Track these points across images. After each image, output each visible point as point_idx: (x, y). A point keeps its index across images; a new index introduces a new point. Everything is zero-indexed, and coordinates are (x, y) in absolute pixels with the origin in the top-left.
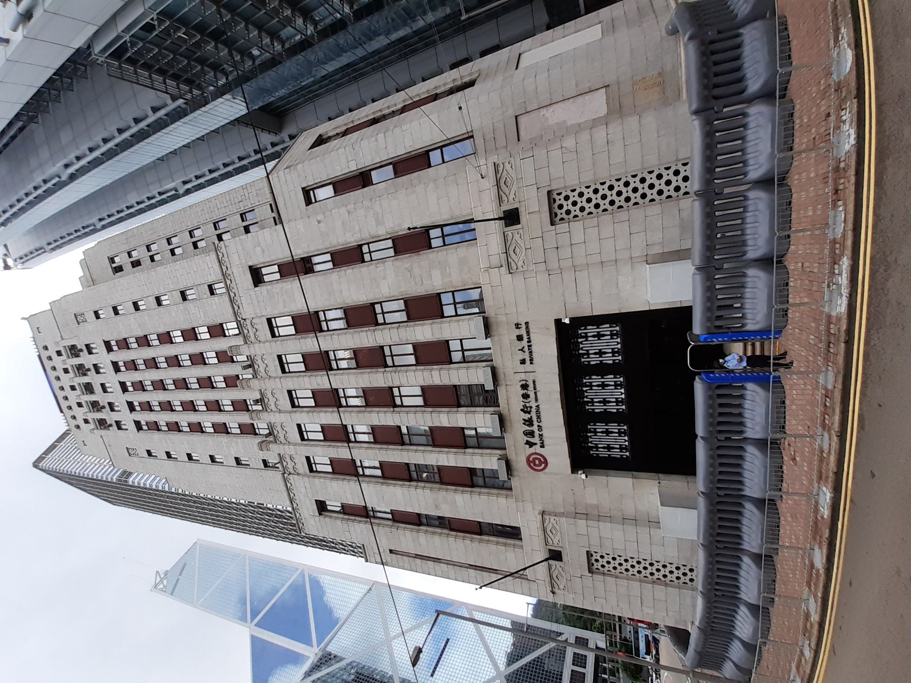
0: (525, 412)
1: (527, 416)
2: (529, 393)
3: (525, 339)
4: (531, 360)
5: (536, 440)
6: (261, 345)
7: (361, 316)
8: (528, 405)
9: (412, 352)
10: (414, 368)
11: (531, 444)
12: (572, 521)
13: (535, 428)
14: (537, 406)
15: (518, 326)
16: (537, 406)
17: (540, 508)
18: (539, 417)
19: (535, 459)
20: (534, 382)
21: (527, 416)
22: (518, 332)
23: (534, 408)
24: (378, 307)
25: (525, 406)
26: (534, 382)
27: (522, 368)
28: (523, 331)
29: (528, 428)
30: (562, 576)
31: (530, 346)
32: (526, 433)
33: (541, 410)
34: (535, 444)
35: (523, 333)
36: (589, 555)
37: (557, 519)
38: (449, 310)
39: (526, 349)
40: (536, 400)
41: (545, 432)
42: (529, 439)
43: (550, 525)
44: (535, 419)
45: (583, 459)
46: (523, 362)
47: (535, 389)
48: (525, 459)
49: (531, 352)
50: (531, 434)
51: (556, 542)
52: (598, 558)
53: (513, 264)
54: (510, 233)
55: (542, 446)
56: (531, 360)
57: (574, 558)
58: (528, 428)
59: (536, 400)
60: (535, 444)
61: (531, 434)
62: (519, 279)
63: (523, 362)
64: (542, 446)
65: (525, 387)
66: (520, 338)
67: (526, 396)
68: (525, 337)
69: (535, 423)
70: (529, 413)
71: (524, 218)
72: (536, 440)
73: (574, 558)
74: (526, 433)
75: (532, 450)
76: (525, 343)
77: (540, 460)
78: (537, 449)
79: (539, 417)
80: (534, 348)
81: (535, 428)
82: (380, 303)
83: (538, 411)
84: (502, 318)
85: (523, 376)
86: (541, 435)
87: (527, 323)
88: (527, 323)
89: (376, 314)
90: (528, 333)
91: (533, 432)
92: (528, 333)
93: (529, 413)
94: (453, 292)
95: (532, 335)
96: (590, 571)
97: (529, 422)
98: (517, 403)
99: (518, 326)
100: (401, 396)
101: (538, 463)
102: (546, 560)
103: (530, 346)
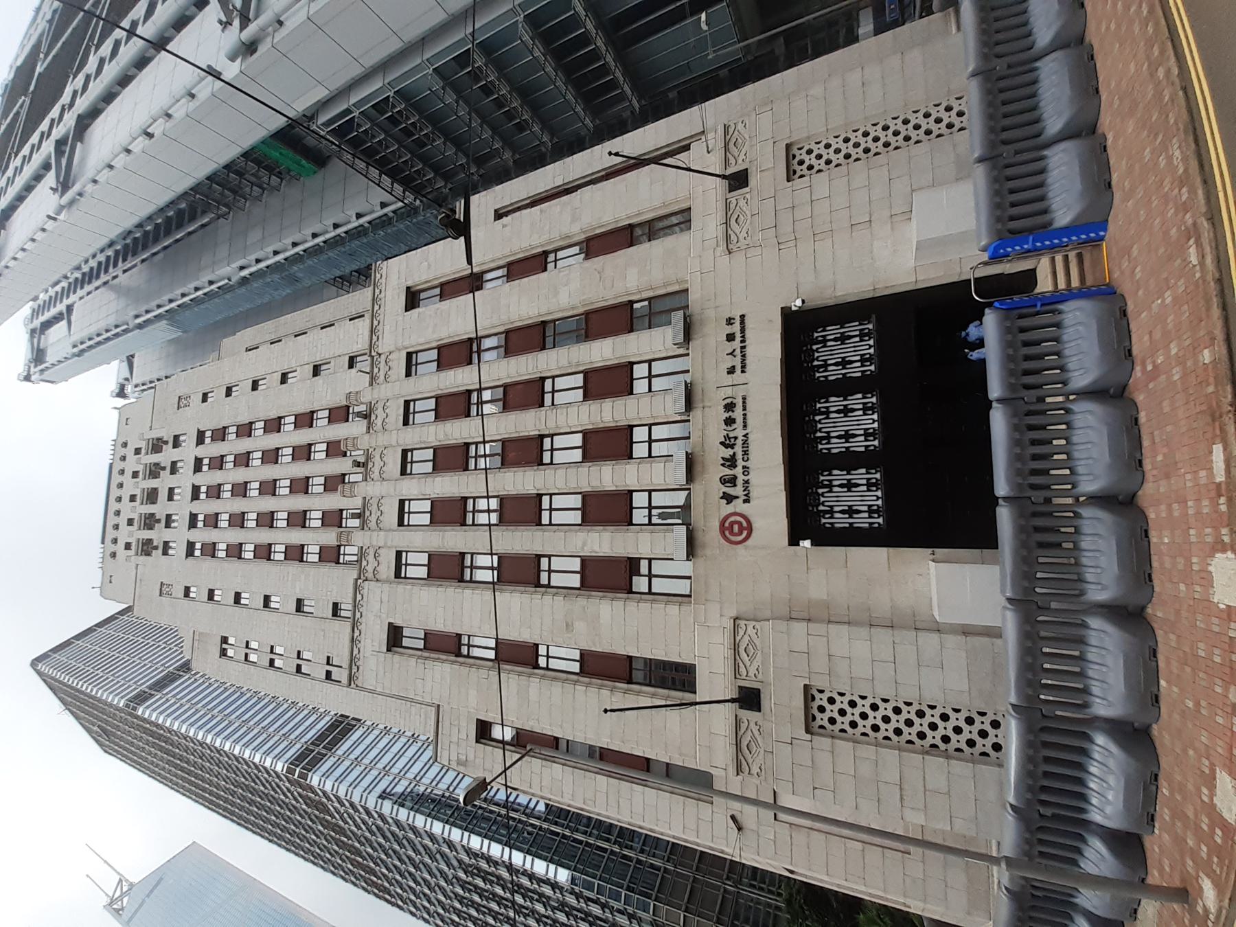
0: (727, 446)
1: (730, 452)
3: (738, 339)
4: (743, 366)
5: (738, 491)
6: (379, 584)
7: (521, 572)
8: (731, 435)
9: (578, 569)
10: (575, 677)
11: (729, 498)
12: (782, 625)
15: (730, 321)
17: (734, 614)
18: (746, 453)
19: (732, 524)
20: (744, 398)
22: (729, 330)
23: (741, 438)
24: (544, 561)
25: (727, 437)
26: (744, 398)
27: (729, 380)
28: (736, 328)
30: (758, 746)
31: (743, 348)
32: (723, 481)
34: (737, 497)
35: (737, 331)
36: (808, 695)
37: (758, 625)
38: (639, 516)
39: (738, 352)
40: (745, 426)
42: (731, 491)
43: (746, 638)
44: (739, 456)
45: (805, 522)
46: (731, 371)
48: (716, 524)
49: (744, 356)
51: (752, 672)
52: (825, 704)
53: (733, 237)
54: (734, 200)
55: (746, 501)
56: (743, 366)
57: (784, 702)
59: (745, 426)
60: (737, 497)
61: (732, 481)
62: (739, 257)
63: (731, 371)
65: (730, 407)
66: (730, 338)
67: (729, 421)
68: (738, 335)
69: (740, 463)
70: (732, 446)
71: (753, 181)
72: (738, 491)
73: (784, 702)
74: (723, 481)
75: (730, 509)
76: (737, 344)
77: (740, 524)
78: (738, 506)
79: (746, 453)
80: (748, 351)
82: (549, 557)
83: (745, 442)
84: (711, 313)
85: (729, 392)
86: (747, 482)
87: (742, 317)
88: (742, 317)
89: (539, 571)
90: (743, 330)
91: (735, 478)
92: (743, 330)
93: (732, 446)
94: (650, 492)
95: (748, 334)
96: (808, 731)
97: (731, 462)
98: (716, 432)
99: (730, 321)
100: (548, 657)
101: (737, 530)
102: (732, 701)
103: (743, 348)
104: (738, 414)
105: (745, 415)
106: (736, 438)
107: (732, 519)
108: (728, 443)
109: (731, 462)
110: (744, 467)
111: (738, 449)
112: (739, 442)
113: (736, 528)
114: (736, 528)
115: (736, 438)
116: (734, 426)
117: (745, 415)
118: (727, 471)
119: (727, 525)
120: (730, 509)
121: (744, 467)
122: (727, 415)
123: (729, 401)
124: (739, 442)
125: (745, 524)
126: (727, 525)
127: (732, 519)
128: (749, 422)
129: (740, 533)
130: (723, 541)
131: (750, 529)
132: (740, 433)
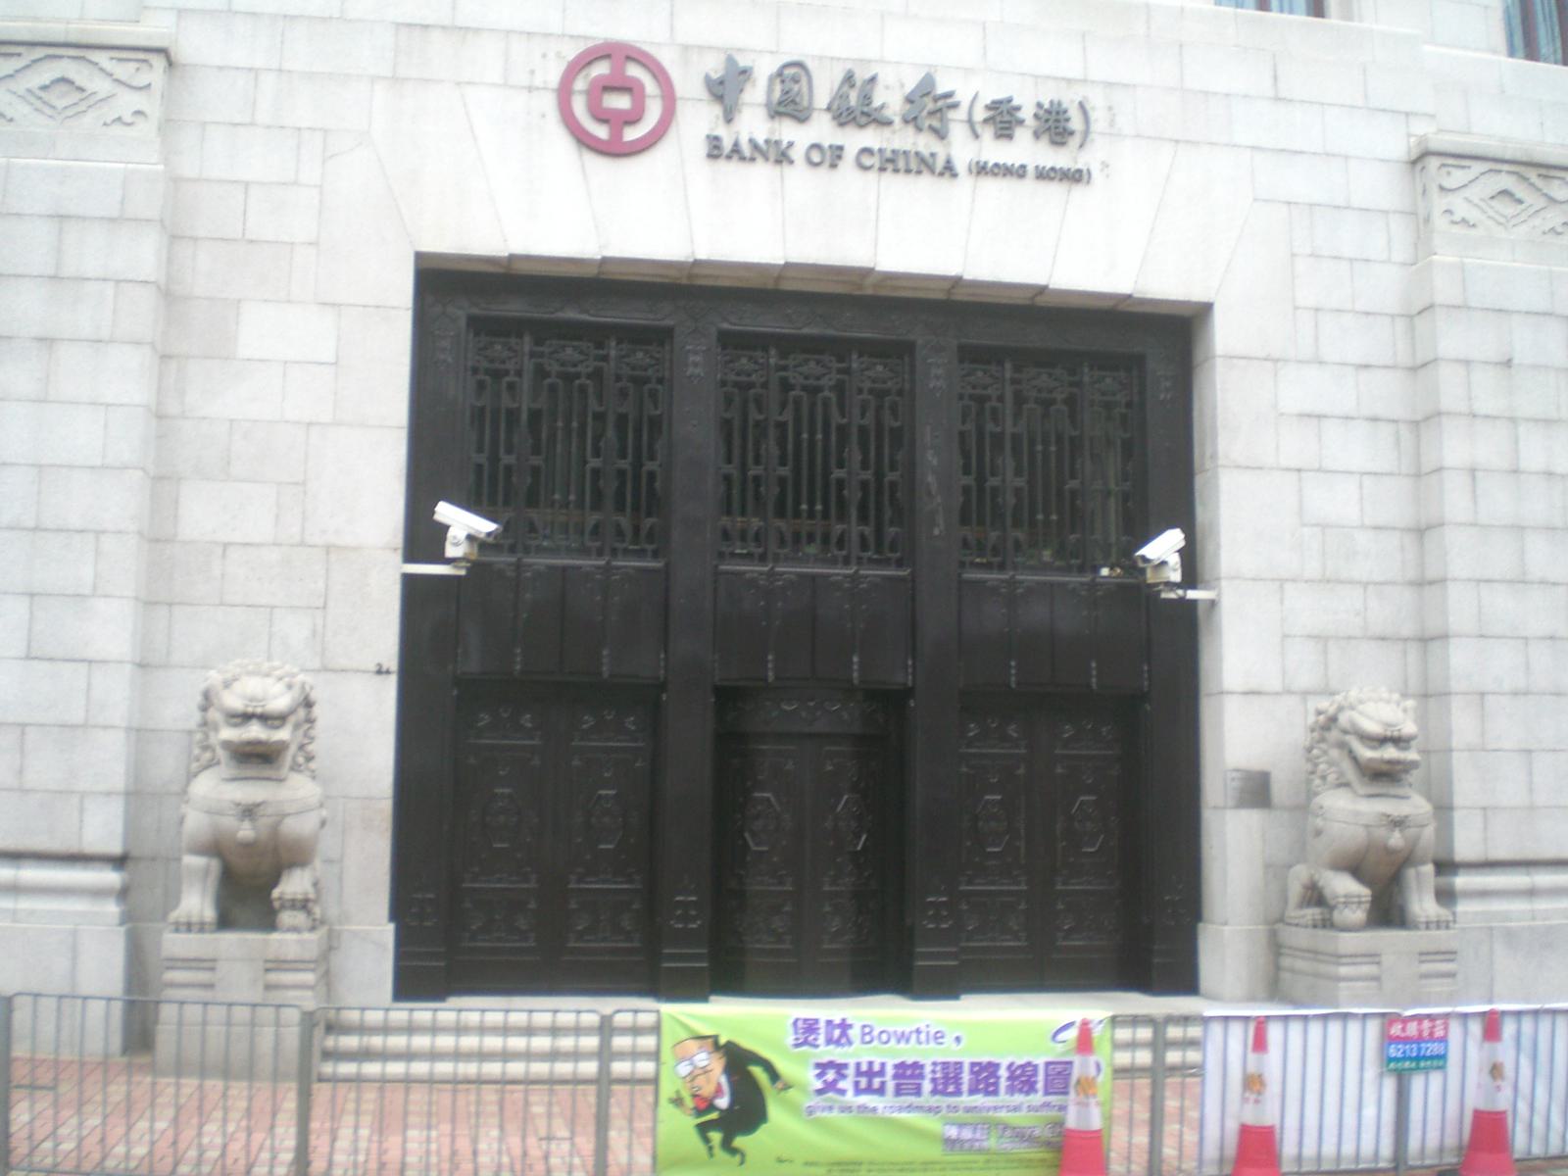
2: (1023, 136)
11: (725, 90)
13: (821, 129)
14: (949, 170)
16: (949, 170)
18: (891, 162)
20: (1074, 177)
21: (890, 98)
25: (945, 104)
29: (822, 96)
33: (926, 181)
34: (729, 118)
40: (981, 170)
41: (798, 177)
42: (756, 94)
47: (1044, 175)
50: (789, 106)
55: (715, 149)
58: (822, 96)
59: (981, 170)
60: (729, 118)
61: (789, 106)
64: (715, 149)
65: (1055, 126)
67: (1003, 119)
69: (855, 140)
72: (753, 124)
77: (633, 118)
78: (697, 119)
81: (821, 129)
83: (924, 165)
86: (781, 156)
104: (1024, 149)
105: (1020, 172)
106: (941, 134)
107: (650, 86)
108: (929, 107)
109: (856, 108)
110: (837, 152)
111: (903, 139)
112: (925, 143)
113: (621, 102)
114: (621, 102)
115: (941, 134)
116: (987, 134)
117: (1020, 172)
118: (823, 92)
119: (634, 71)
120: (689, 84)
121: (837, 152)
122: (1027, 113)
123: (1076, 123)
124: (925, 143)
125: (632, 134)
126: (634, 71)
127: (650, 86)
128: (991, 186)
129: (601, 116)
130: (571, 52)
131: (615, 150)
132: (962, 148)
